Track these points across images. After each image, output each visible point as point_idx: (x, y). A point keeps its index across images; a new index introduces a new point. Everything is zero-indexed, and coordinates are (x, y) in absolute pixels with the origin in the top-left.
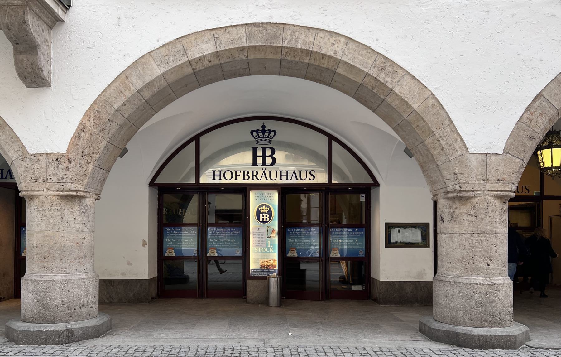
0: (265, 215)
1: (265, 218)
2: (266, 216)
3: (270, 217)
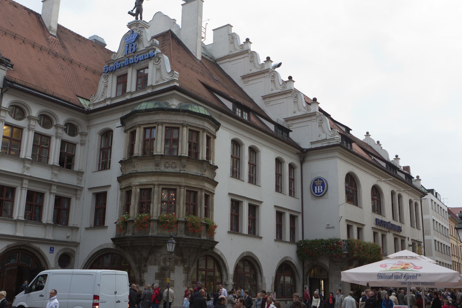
0: (319, 187)
1: (319, 189)
2: (320, 188)
3: (323, 189)
